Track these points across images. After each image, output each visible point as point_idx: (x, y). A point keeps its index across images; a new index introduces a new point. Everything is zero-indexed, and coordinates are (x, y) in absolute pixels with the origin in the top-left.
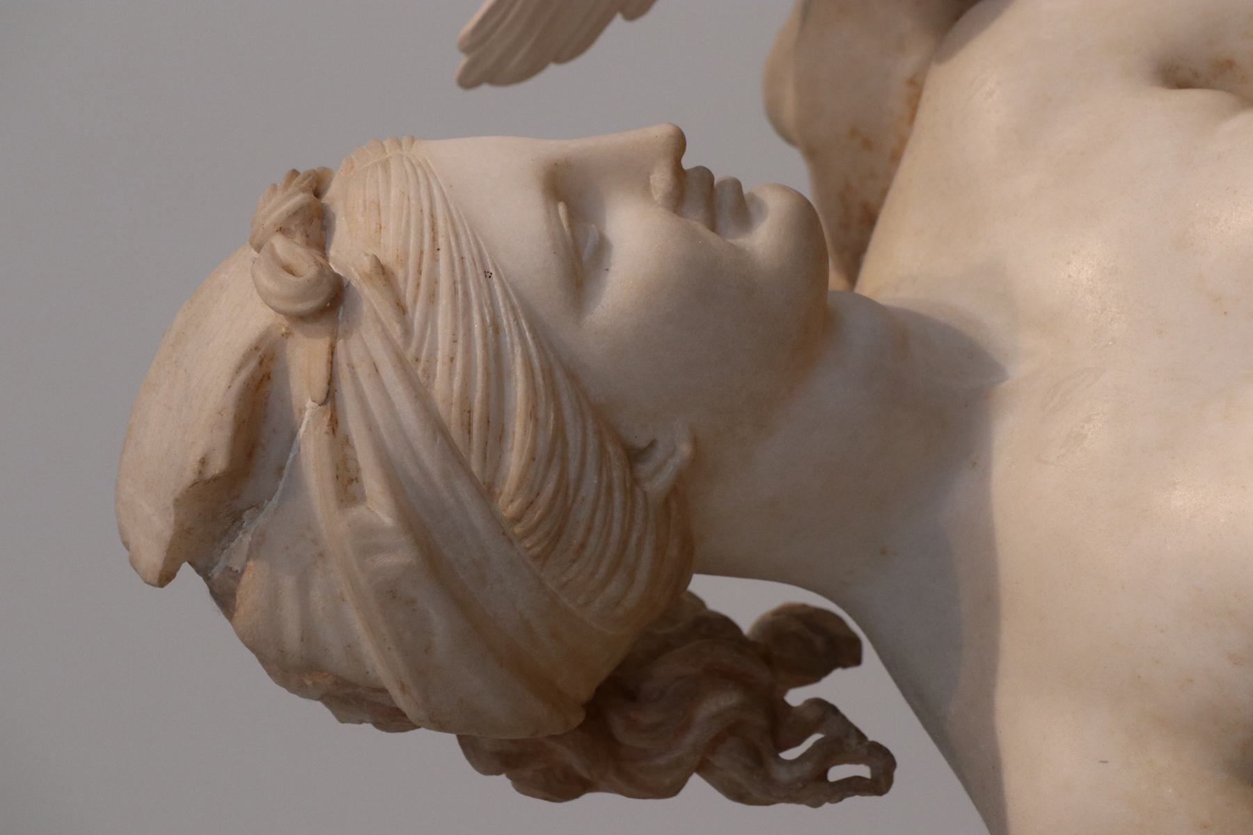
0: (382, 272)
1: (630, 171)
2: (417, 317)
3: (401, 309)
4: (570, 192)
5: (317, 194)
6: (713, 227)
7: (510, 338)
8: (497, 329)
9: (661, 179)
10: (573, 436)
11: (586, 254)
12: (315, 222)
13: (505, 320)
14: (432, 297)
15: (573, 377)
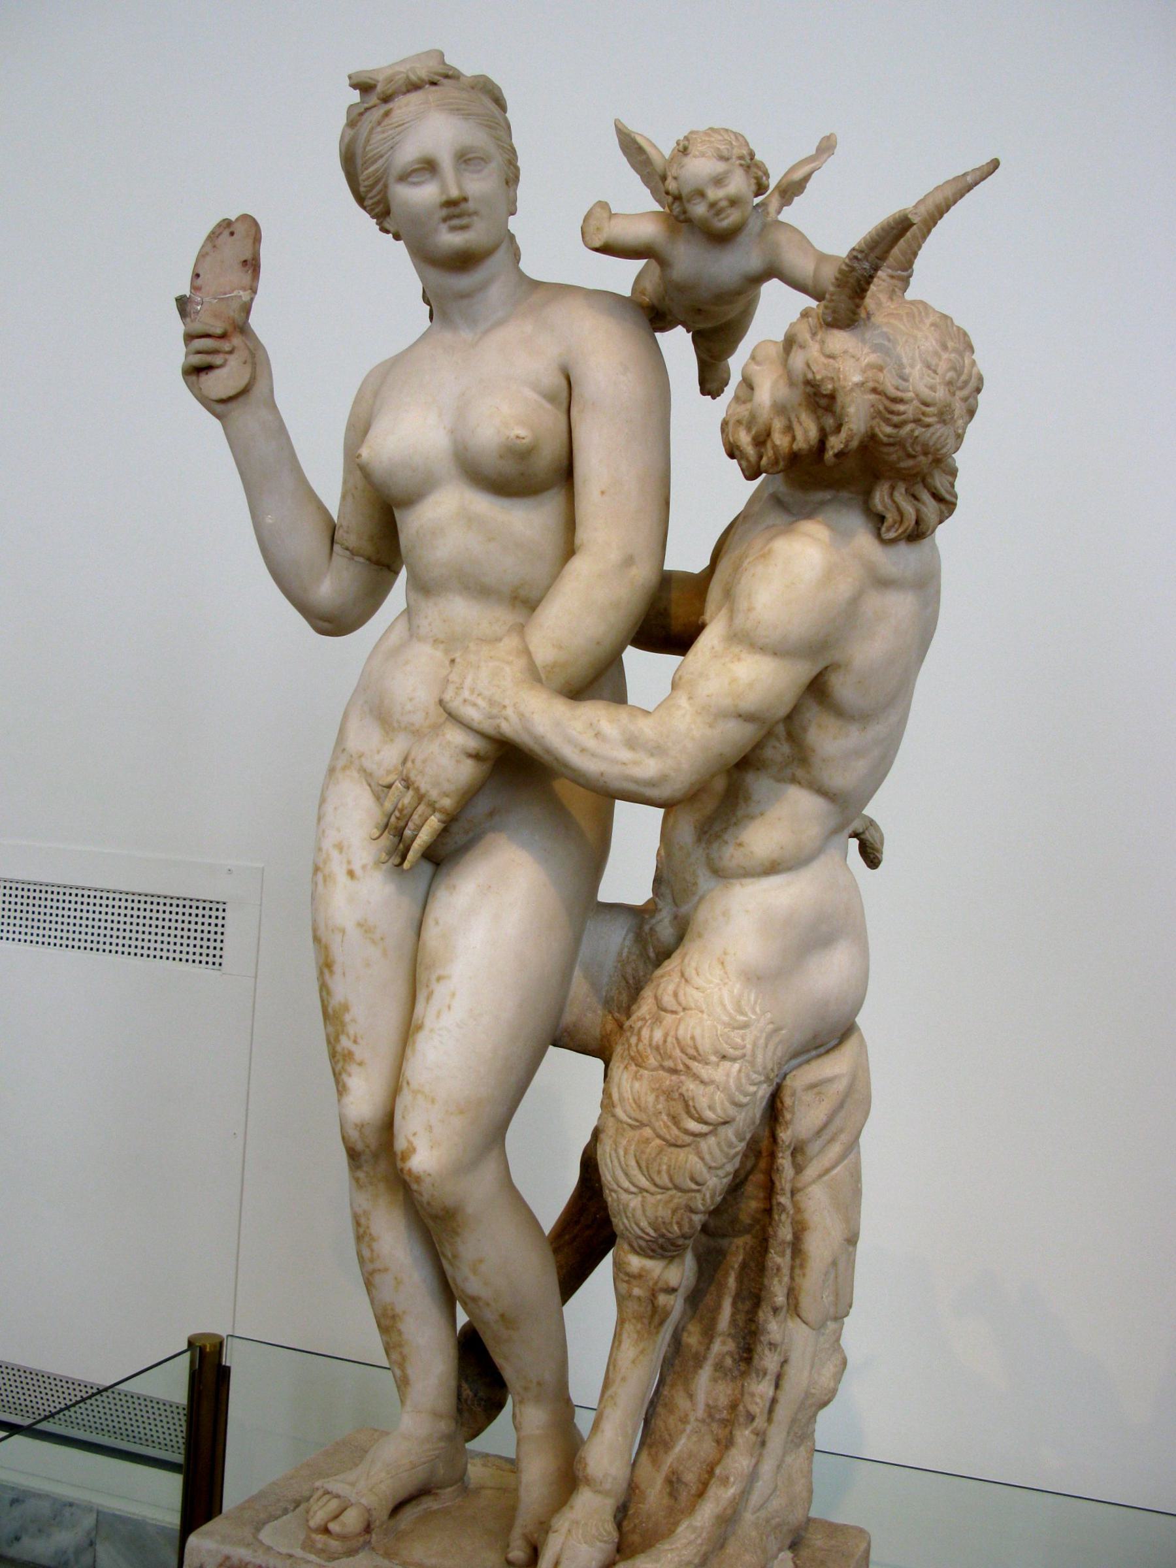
0: (387, 114)
1: (444, 188)
2: (379, 129)
3: (379, 123)
4: (429, 167)
5: (434, 84)
6: (445, 220)
7: (380, 162)
8: (382, 156)
9: (444, 198)
10: (374, 192)
11: (410, 179)
12: (414, 86)
13: (384, 159)
14: (383, 132)
15: (386, 186)
